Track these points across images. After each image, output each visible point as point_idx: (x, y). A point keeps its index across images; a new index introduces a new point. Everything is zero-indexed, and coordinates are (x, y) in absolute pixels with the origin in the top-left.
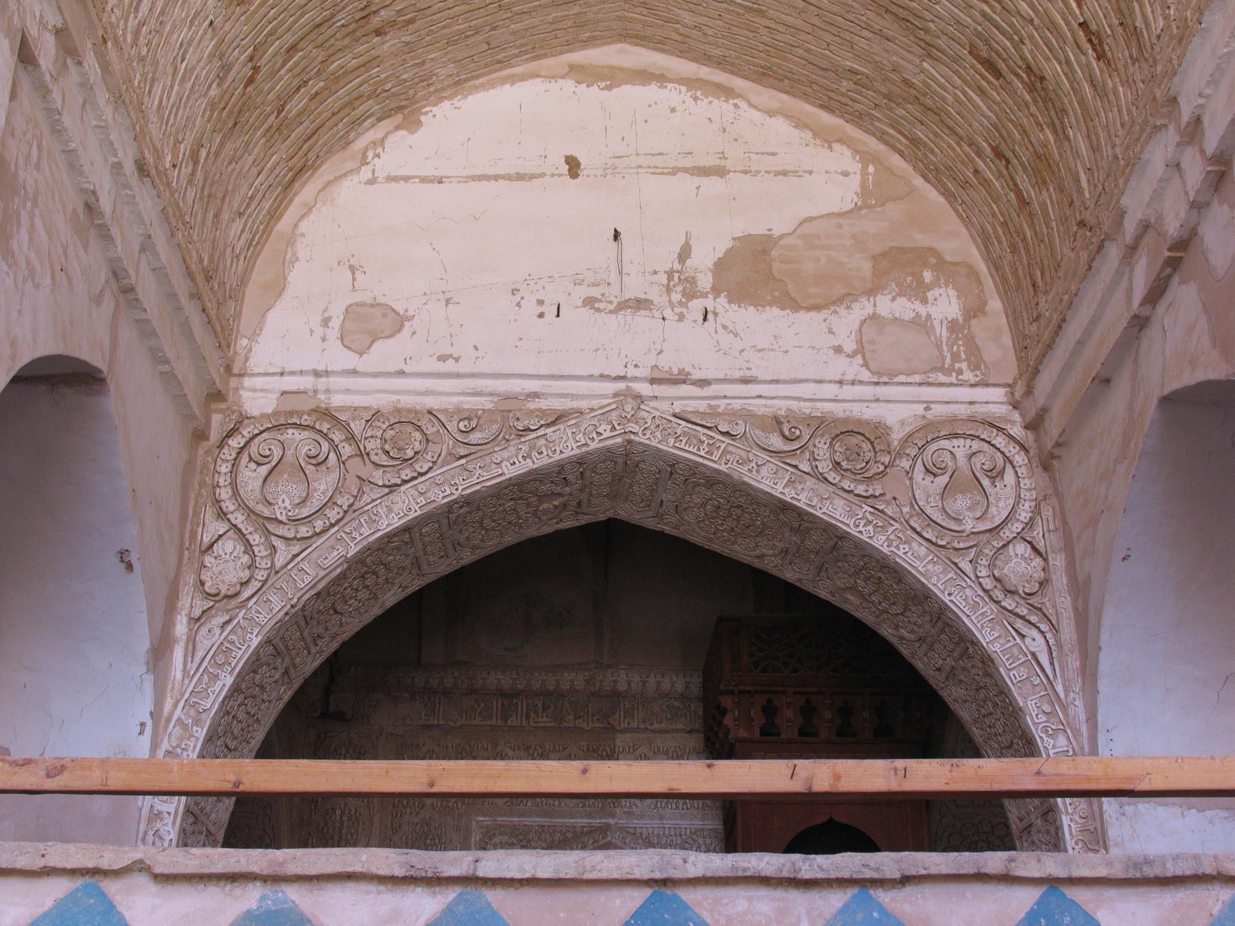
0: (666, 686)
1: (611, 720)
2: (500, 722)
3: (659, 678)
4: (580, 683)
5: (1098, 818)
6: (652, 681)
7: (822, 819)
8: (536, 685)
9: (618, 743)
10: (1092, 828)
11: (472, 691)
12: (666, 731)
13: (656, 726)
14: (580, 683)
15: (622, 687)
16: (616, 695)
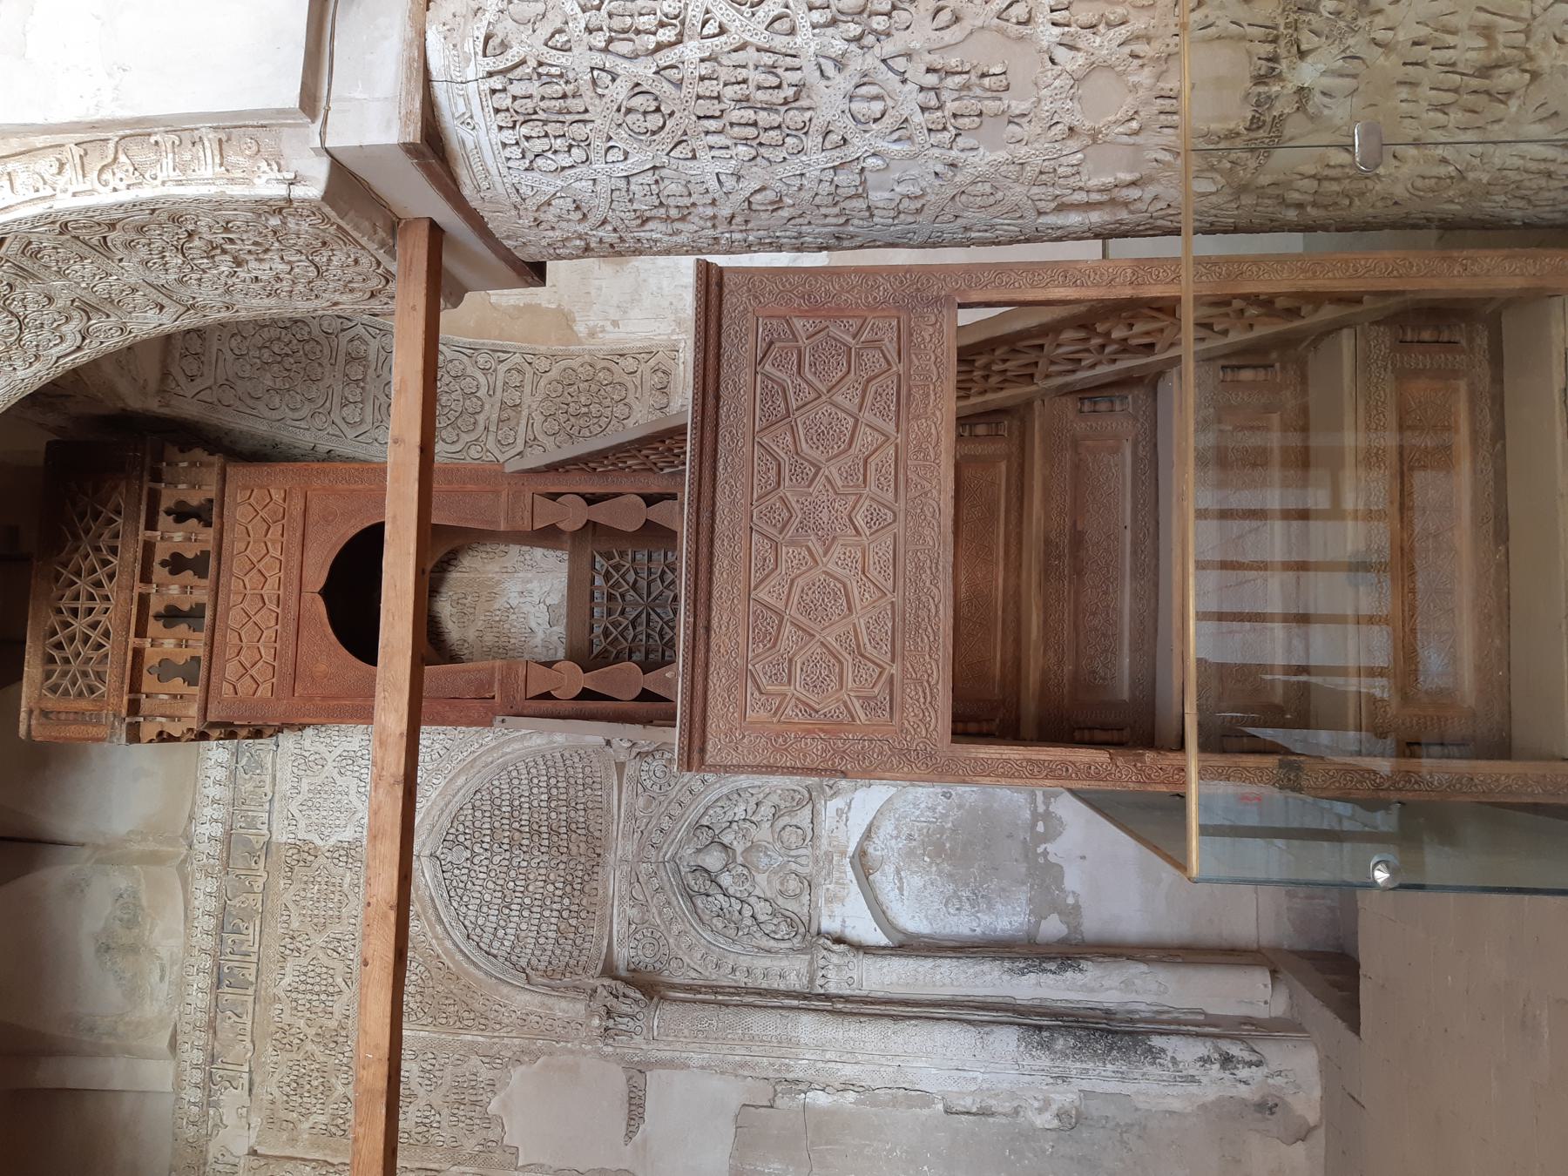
0: (220, 774)
1: (258, 847)
2: (251, 991)
3: (210, 782)
4: (211, 886)
5: (58, 139)
6: (214, 791)
7: (321, 607)
8: (209, 942)
9: (284, 840)
10: (78, 151)
11: (212, 1027)
12: (274, 777)
13: (268, 789)
14: (211, 886)
15: (218, 830)
16: (228, 839)
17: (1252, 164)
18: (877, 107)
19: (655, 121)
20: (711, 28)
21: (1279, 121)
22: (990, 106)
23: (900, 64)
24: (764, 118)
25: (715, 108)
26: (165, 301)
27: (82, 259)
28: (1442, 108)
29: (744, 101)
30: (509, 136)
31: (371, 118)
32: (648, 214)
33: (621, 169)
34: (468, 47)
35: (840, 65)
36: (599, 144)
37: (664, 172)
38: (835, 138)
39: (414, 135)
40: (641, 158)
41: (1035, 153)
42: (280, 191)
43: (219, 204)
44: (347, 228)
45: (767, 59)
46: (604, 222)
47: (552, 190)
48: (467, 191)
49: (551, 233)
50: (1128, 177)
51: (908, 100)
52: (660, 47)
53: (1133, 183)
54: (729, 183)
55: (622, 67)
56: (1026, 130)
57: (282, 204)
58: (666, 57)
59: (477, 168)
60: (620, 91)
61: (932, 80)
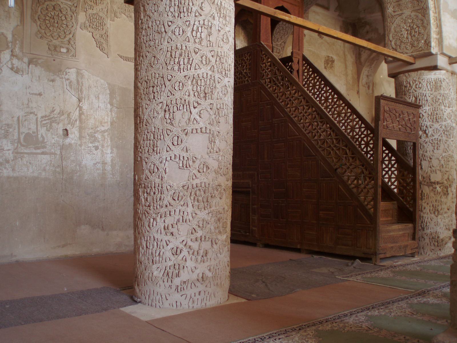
17: (425, 183)
18: (435, 132)
19: (434, 101)
20: (445, 111)
21: (432, 186)
22: (436, 148)
23: (441, 135)
24: (435, 117)
25: (436, 110)
26: (396, 13)
27: (414, 7)
28: (433, 206)
29: (437, 114)
30: (433, 80)
31: (442, 62)
32: (418, 98)
33: (427, 95)
34: (444, 76)
35: (441, 127)
36: (431, 93)
37: (426, 102)
38: (432, 126)
39: (438, 67)
40: (429, 99)
41: (428, 154)
42: (432, 46)
43: (429, 35)
44: (421, 52)
45: (442, 117)
46: (415, 91)
47: (424, 84)
48: (423, 71)
49: (411, 82)
50: (423, 167)
51: (436, 137)
52: (443, 103)
53: (421, 168)
54: (425, 111)
55: (441, 97)
56: (431, 153)
57: (429, 45)
58: (442, 103)
59: (428, 74)
60: (439, 97)
61: (439, 140)
